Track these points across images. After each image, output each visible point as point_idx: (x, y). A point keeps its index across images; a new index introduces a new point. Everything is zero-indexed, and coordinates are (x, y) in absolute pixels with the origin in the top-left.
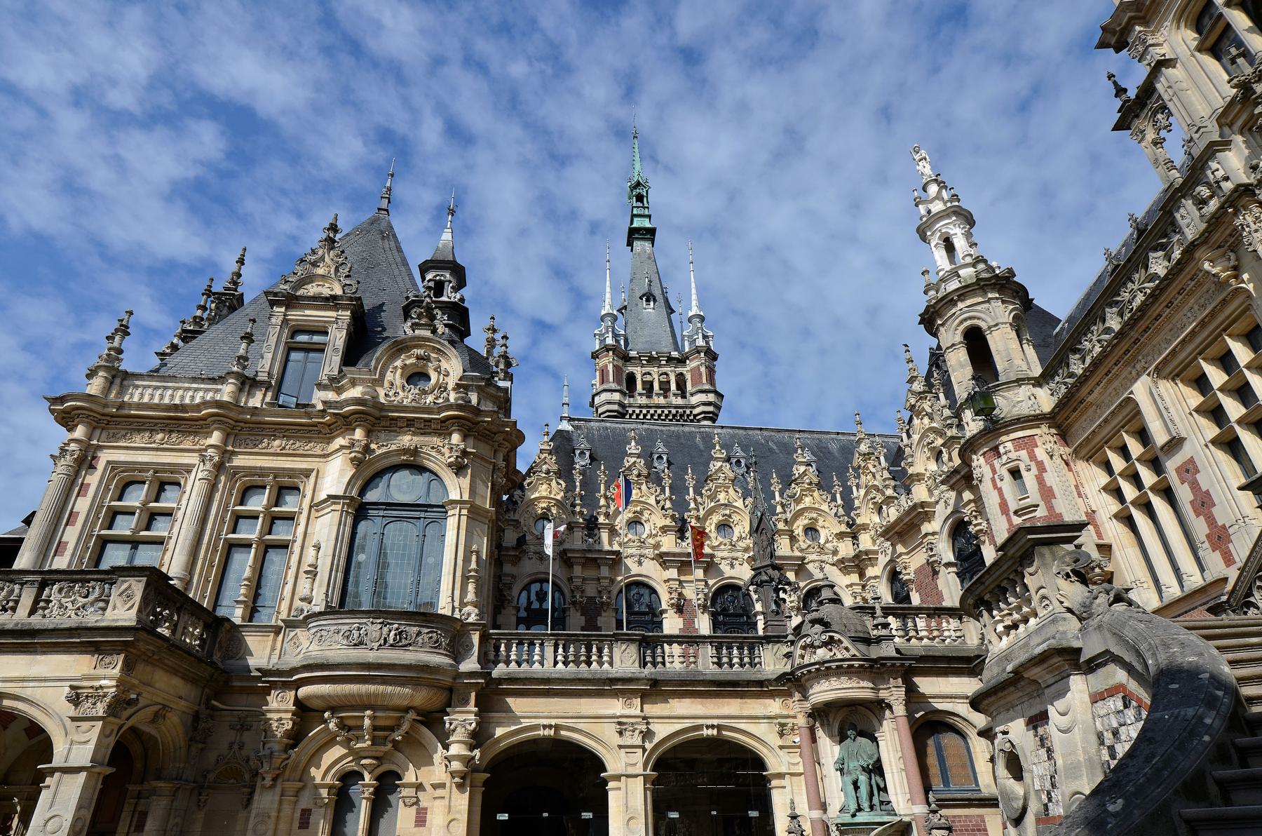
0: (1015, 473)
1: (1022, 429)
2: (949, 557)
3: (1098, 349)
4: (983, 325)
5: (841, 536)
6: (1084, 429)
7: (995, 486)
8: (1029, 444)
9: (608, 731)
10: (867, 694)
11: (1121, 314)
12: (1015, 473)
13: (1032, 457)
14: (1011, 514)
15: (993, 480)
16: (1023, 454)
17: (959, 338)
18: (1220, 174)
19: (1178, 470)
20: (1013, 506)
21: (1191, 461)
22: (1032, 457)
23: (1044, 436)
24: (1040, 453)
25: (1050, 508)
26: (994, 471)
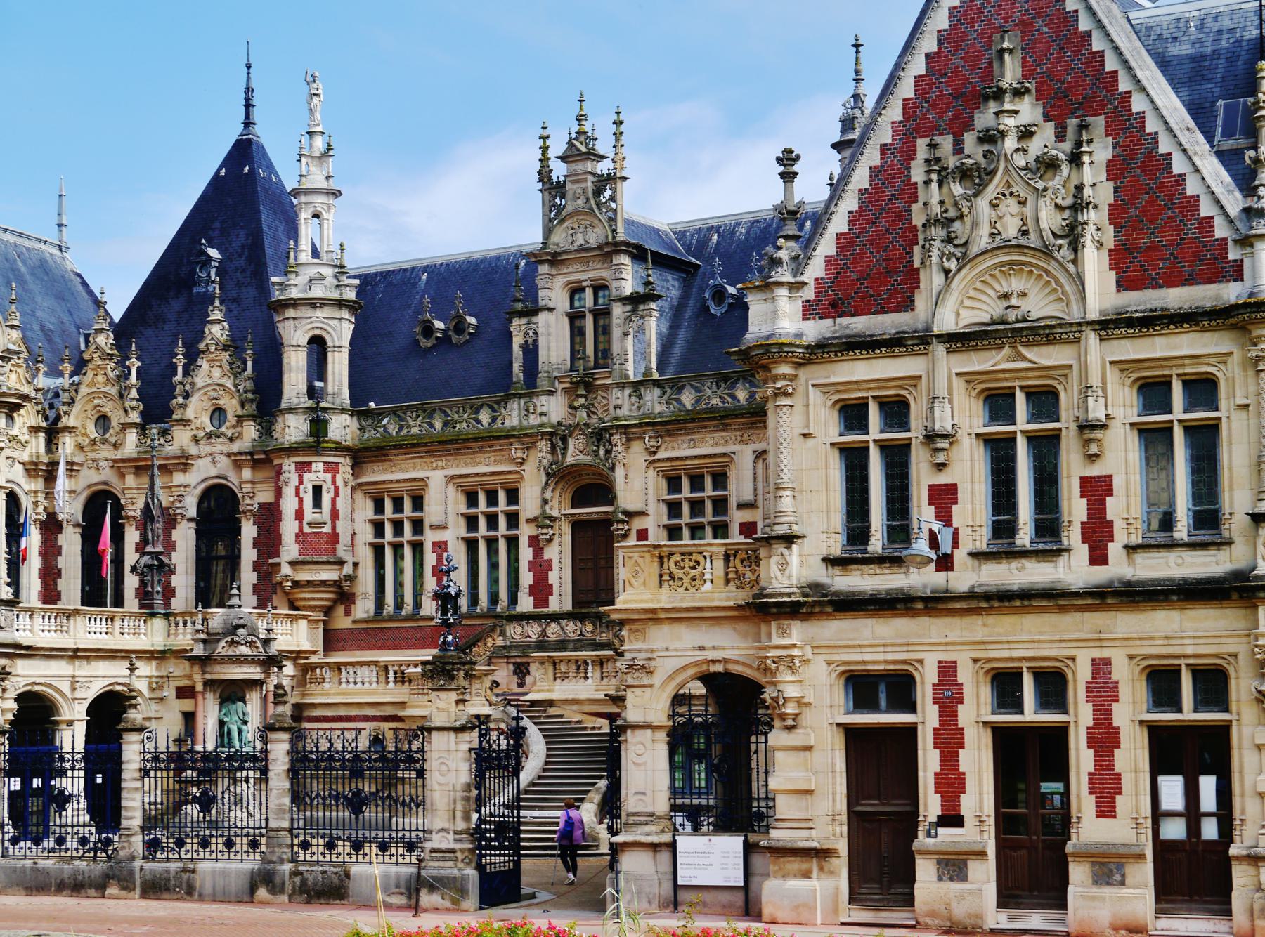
0: (317, 490)
1: (335, 455)
2: (192, 512)
3: (415, 430)
4: (329, 343)
5: (35, 430)
6: (377, 474)
7: (297, 494)
8: (332, 469)
9: (65, 686)
10: (258, 677)
11: (446, 424)
12: (317, 490)
13: (334, 482)
14: (305, 522)
15: (297, 489)
16: (329, 476)
17: (304, 341)
18: (544, 409)
19: (434, 543)
20: (309, 515)
21: (445, 543)
22: (334, 482)
23: (345, 463)
24: (339, 482)
25: (334, 528)
26: (301, 482)
